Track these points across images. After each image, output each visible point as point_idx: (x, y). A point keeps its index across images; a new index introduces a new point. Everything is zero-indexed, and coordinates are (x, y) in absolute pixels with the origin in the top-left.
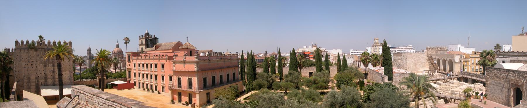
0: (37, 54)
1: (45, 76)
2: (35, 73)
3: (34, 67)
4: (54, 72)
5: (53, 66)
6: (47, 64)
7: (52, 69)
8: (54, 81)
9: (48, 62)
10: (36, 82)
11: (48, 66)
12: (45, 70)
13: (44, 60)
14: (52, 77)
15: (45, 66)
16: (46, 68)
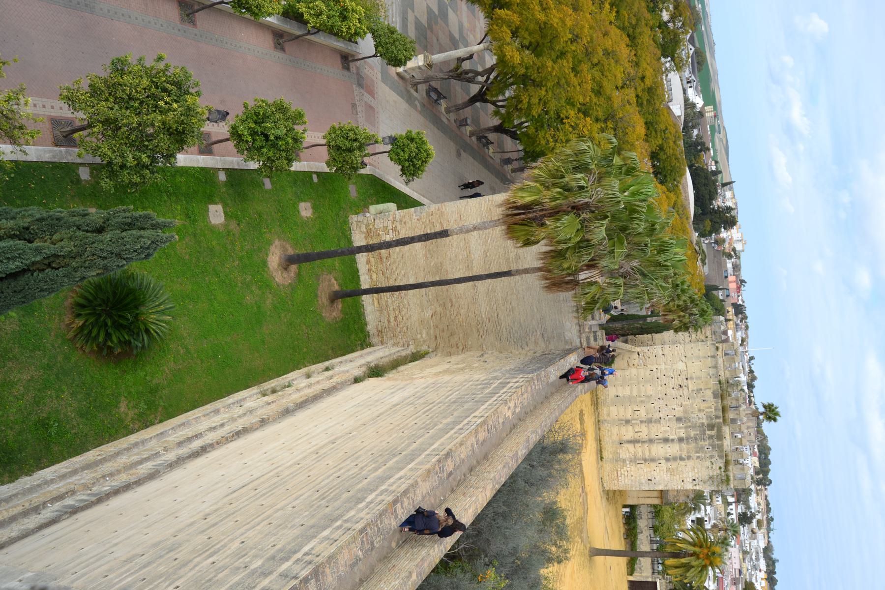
0: (706, 399)
1: (653, 420)
2: (660, 396)
3: (674, 393)
4: (666, 440)
5: (681, 440)
6: (685, 425)
7: (671, 437)
8: (644, 442)
9: (690, 427)
10: (640, 397)
11: (678, 425)
12: (669, 420)
13: (693, 415)
14: (653, 436)
15: (679, 420)
16: (675, 422)
